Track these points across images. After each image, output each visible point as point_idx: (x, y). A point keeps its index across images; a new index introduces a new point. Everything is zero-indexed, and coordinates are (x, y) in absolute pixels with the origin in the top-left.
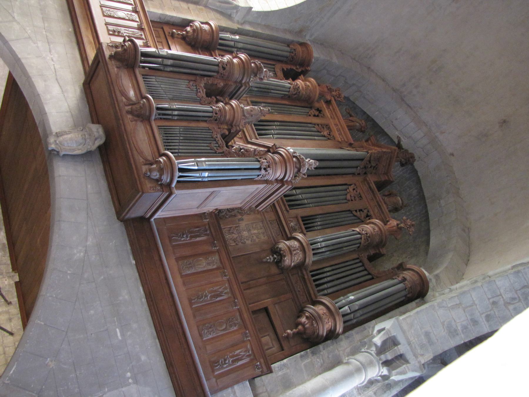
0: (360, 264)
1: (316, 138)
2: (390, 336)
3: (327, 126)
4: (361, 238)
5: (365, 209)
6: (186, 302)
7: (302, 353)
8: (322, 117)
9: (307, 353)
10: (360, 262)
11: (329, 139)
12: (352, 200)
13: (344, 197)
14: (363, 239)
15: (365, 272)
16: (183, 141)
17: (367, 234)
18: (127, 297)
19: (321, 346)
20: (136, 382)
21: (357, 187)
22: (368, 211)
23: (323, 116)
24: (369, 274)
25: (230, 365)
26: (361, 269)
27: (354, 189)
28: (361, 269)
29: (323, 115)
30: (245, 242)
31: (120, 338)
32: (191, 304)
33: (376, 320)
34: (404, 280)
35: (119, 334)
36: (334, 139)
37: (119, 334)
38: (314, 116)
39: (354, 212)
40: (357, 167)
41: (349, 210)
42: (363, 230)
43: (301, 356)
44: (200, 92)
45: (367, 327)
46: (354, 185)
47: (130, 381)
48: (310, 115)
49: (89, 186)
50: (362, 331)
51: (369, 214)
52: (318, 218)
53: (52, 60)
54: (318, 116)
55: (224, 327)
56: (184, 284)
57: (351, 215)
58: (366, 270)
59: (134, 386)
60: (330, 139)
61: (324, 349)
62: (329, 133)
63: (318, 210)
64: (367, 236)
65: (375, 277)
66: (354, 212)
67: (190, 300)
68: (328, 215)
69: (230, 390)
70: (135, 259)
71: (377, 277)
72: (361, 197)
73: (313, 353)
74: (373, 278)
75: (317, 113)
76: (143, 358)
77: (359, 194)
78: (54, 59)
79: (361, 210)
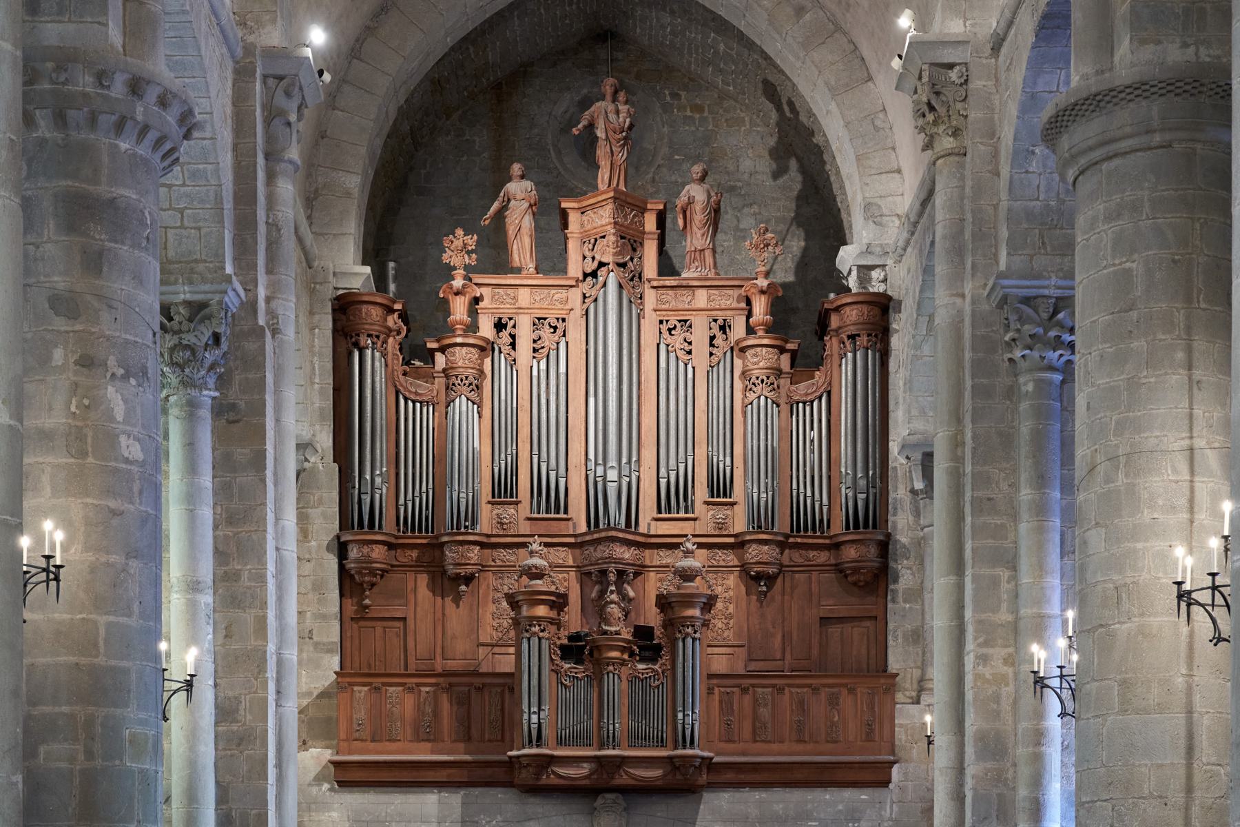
0: (801, 405)
1: (562, 369)
2: (920, 462)
3: (534, 325)
4: (766, 398)
5: (710, 329)
6: (801, 747)
7: (889, 598)
8: (514, 327)
9: (892, 590)
10: (798, 403)
11: (564, 335)
12: (689, 352)
13: (681, 365)
14: (768, 394)
15: (815, 404)
16: (648, 720)
17: (762, 381)
18: (781, 806)
19: (892, 564)
20: (859, 820)
21: (667, 321)
22: (715, 321)
23: (512, 322)
24: (820, 398)
25: (874, 720)
26: (808, 409)
27: (670, 330)
28: (808, 409)
29: (510, 319)
30: (730, 614)
31: (817, 823)
32: (805, 742)
33: (890, 438)
34: (852, 337)
35: (814, 824)
36: (564, 320)
37: (814, 824)
38: (513, 345)
39: (715, 360)
40: (631, 302)
41: (708, 372)
42: (754, 384)
43: (894, 601)
44: (576, 673)
45: (894, 464)
46: (661, 326)
47: (856, 825)
48: (514, 360)
49: (659, 814)
50: (896, 477)
51: (720, 322)
52: (712, 455)
53: (490, 822)
54: (513, 337)
55: (836, 713)
56: (782, 742)
57: (715, 369)
58: (812, 402)
59: (862, 822)
60: (564, 331)
61: (896, 561)
62: (552, 330)
63: (701, 452)
64: (767, 383)
65: (829, 389)
66: (715, 360)
67: (800, 741)
68: (710, 430)
69: (896, 729)
70: (745, 788)
71: (830, 384)
72: (686, 321)
73: (896, 581)
74: (829, 393)
75: (505, 334)
76: (840, 807)
77: (680, 321)
78: (488, 819)
79: (712, 338)
